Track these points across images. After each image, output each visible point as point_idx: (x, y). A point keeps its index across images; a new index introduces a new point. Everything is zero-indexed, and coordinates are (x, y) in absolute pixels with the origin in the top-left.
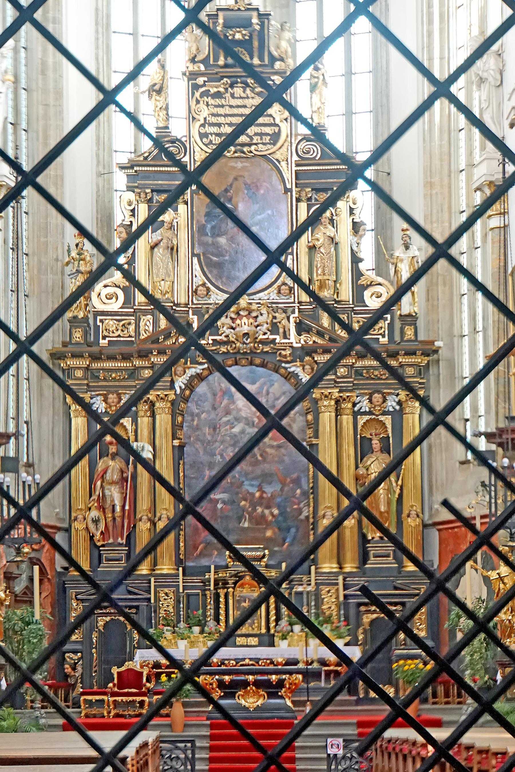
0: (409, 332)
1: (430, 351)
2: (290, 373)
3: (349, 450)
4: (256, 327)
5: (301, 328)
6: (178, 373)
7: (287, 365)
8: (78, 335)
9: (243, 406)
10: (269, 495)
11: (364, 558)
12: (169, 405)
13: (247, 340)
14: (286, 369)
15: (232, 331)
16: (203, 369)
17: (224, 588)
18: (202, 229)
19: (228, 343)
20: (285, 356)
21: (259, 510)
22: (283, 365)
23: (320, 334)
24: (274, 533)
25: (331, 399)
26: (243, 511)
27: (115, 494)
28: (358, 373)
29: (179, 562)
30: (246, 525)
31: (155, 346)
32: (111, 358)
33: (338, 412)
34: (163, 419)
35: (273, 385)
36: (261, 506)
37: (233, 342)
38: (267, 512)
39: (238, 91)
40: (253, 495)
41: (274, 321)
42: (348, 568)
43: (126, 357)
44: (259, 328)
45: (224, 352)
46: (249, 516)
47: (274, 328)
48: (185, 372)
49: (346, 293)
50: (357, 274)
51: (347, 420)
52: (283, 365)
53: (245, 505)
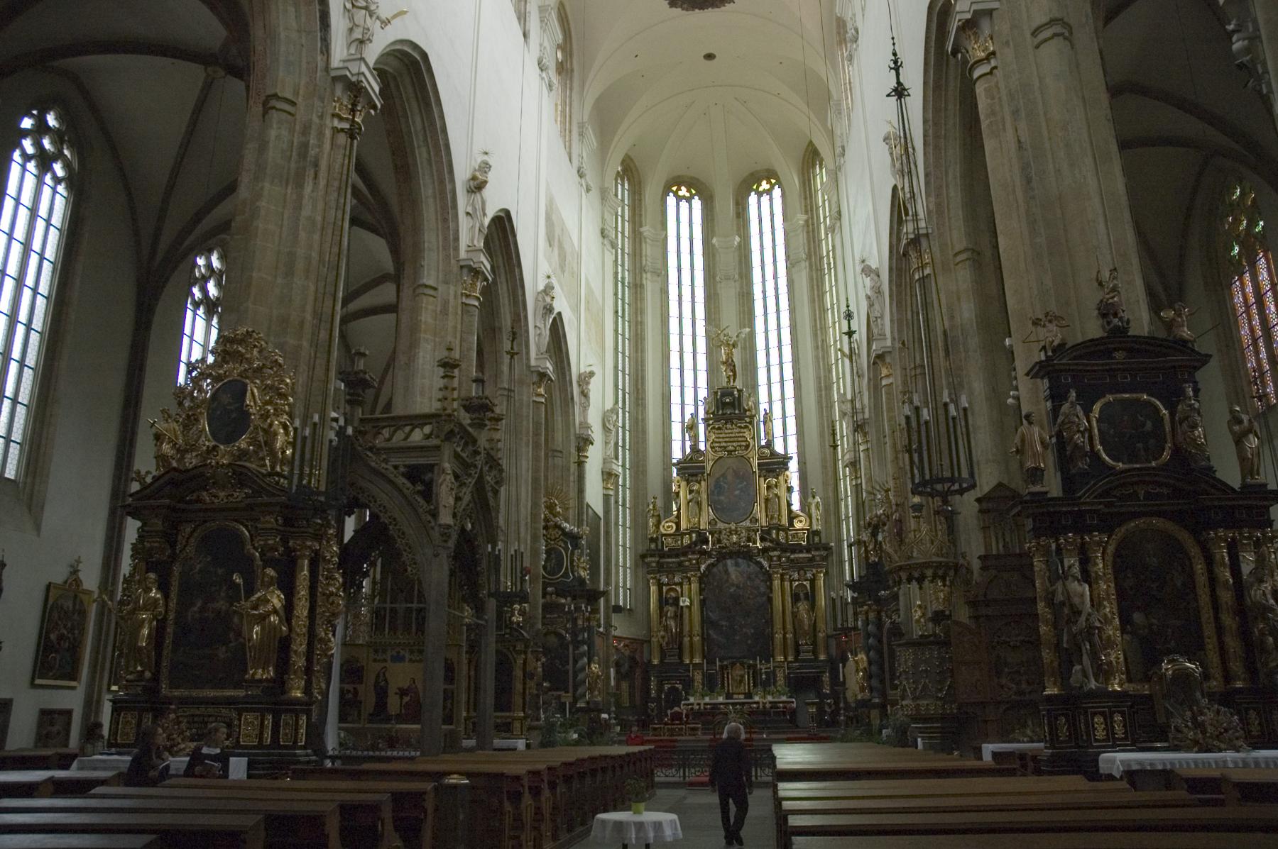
0: (817, 539)
1: (827, 548)
3: (789, 599)
5: (762, 539)
8: (653, 546)
11: (797, 652)
18: (713, 492)
19: (726, 547)
23: (771, 541)
27: (672, 623)
28: (792, 560)
29: (704, 657)
32: (669, 557)
33: (782, 580)
34: (695, 586)
39: (729, 426)
42: (790, 658)
43: (677, 556)
47: (749, 540)
49: (785, 521)
50: (790, 511)
51: (787, 584)
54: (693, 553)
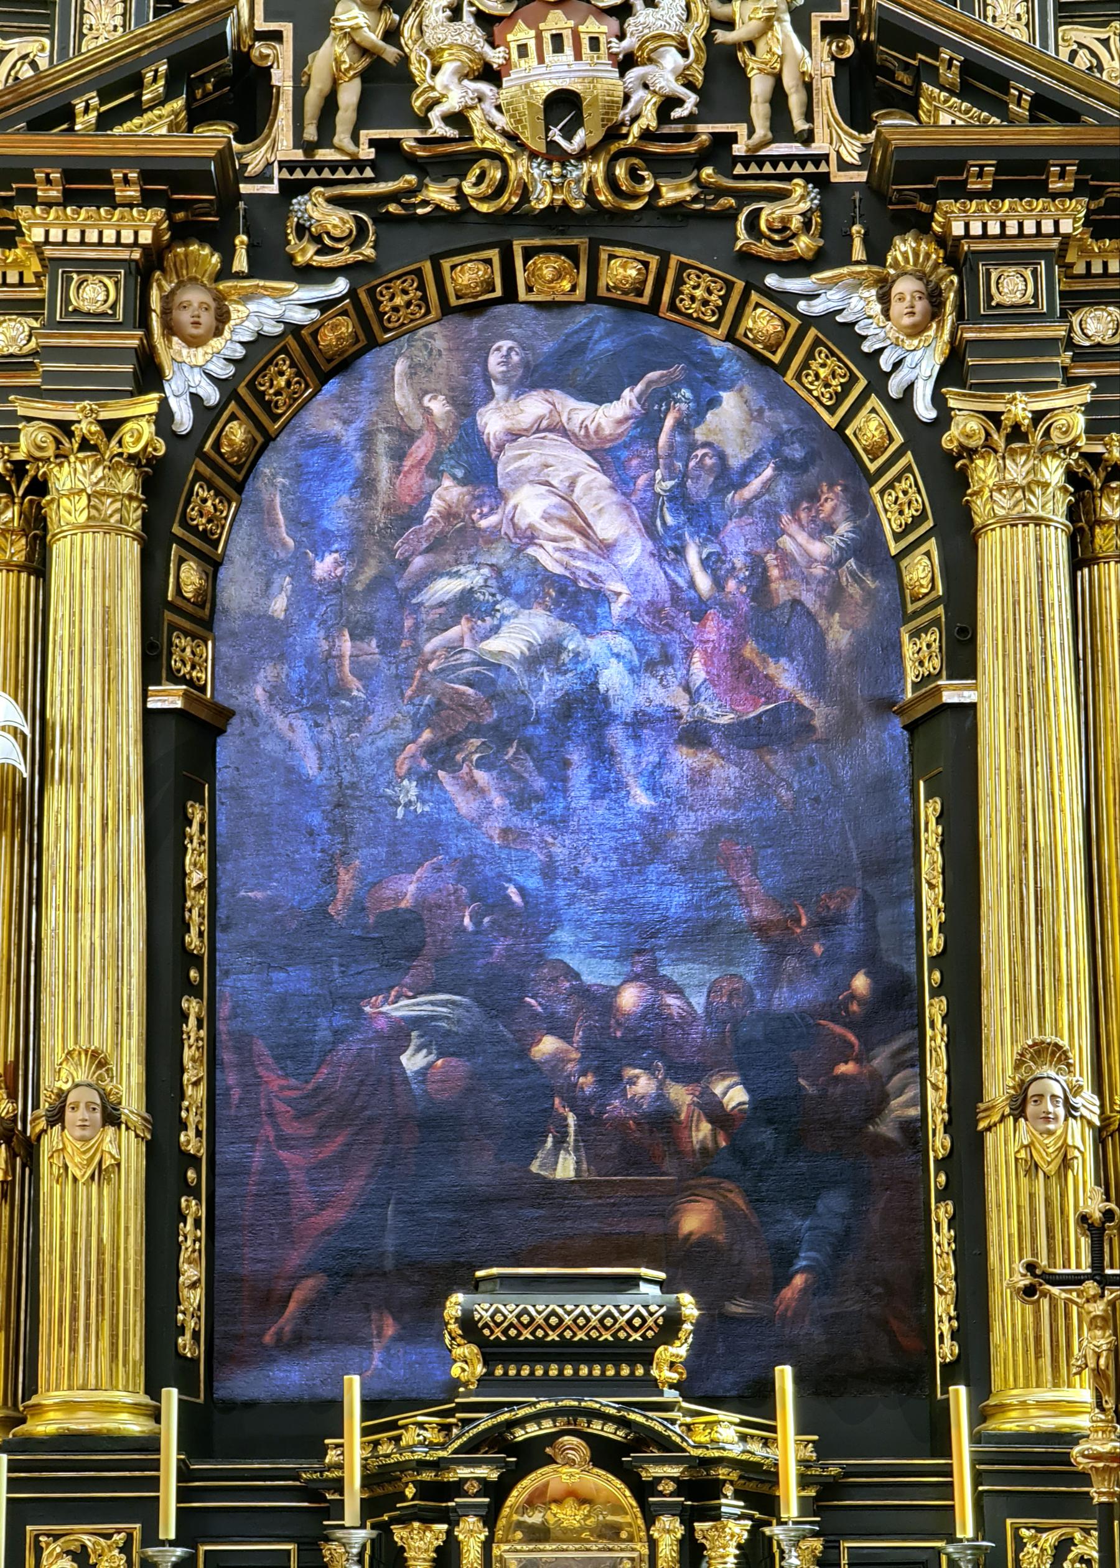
2: (807, 321)
4: (626, 63)
6: (184, 317)
7: (794, 285)
9: (547, 517)
10: (698, 1002)
12: (128, 481)
13: (568, 135)
14: (786, 300)
15: (485, 88)
16: (324, 306)
17: (428, 1518)
20: (784, 234)
21: (643, 1085)
22: (772, 280)
24: (727, 1213)
25: (1043, 452)
26: (550, 1092)
30: (566, 1168)
31: (49, 144)
35: (714, 403)
36: (649, 1068)
37: (495, 155)
38: (681, 1095)
40: (602, 1002)
41: (722, 36)
44: (634, 73)
45: (439, 215)
46: (584, 1120)
48: (222, 317)
52: (772, 280)
53: (558, 1059)
54: (86, 185)
